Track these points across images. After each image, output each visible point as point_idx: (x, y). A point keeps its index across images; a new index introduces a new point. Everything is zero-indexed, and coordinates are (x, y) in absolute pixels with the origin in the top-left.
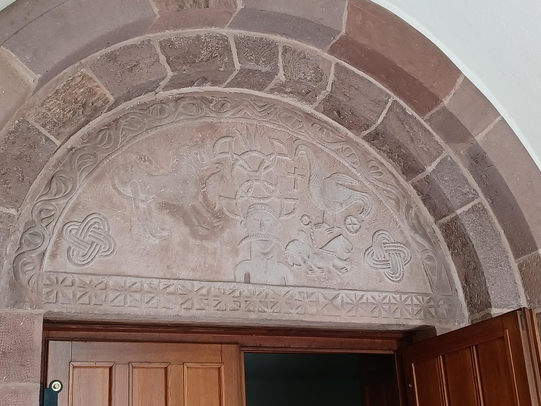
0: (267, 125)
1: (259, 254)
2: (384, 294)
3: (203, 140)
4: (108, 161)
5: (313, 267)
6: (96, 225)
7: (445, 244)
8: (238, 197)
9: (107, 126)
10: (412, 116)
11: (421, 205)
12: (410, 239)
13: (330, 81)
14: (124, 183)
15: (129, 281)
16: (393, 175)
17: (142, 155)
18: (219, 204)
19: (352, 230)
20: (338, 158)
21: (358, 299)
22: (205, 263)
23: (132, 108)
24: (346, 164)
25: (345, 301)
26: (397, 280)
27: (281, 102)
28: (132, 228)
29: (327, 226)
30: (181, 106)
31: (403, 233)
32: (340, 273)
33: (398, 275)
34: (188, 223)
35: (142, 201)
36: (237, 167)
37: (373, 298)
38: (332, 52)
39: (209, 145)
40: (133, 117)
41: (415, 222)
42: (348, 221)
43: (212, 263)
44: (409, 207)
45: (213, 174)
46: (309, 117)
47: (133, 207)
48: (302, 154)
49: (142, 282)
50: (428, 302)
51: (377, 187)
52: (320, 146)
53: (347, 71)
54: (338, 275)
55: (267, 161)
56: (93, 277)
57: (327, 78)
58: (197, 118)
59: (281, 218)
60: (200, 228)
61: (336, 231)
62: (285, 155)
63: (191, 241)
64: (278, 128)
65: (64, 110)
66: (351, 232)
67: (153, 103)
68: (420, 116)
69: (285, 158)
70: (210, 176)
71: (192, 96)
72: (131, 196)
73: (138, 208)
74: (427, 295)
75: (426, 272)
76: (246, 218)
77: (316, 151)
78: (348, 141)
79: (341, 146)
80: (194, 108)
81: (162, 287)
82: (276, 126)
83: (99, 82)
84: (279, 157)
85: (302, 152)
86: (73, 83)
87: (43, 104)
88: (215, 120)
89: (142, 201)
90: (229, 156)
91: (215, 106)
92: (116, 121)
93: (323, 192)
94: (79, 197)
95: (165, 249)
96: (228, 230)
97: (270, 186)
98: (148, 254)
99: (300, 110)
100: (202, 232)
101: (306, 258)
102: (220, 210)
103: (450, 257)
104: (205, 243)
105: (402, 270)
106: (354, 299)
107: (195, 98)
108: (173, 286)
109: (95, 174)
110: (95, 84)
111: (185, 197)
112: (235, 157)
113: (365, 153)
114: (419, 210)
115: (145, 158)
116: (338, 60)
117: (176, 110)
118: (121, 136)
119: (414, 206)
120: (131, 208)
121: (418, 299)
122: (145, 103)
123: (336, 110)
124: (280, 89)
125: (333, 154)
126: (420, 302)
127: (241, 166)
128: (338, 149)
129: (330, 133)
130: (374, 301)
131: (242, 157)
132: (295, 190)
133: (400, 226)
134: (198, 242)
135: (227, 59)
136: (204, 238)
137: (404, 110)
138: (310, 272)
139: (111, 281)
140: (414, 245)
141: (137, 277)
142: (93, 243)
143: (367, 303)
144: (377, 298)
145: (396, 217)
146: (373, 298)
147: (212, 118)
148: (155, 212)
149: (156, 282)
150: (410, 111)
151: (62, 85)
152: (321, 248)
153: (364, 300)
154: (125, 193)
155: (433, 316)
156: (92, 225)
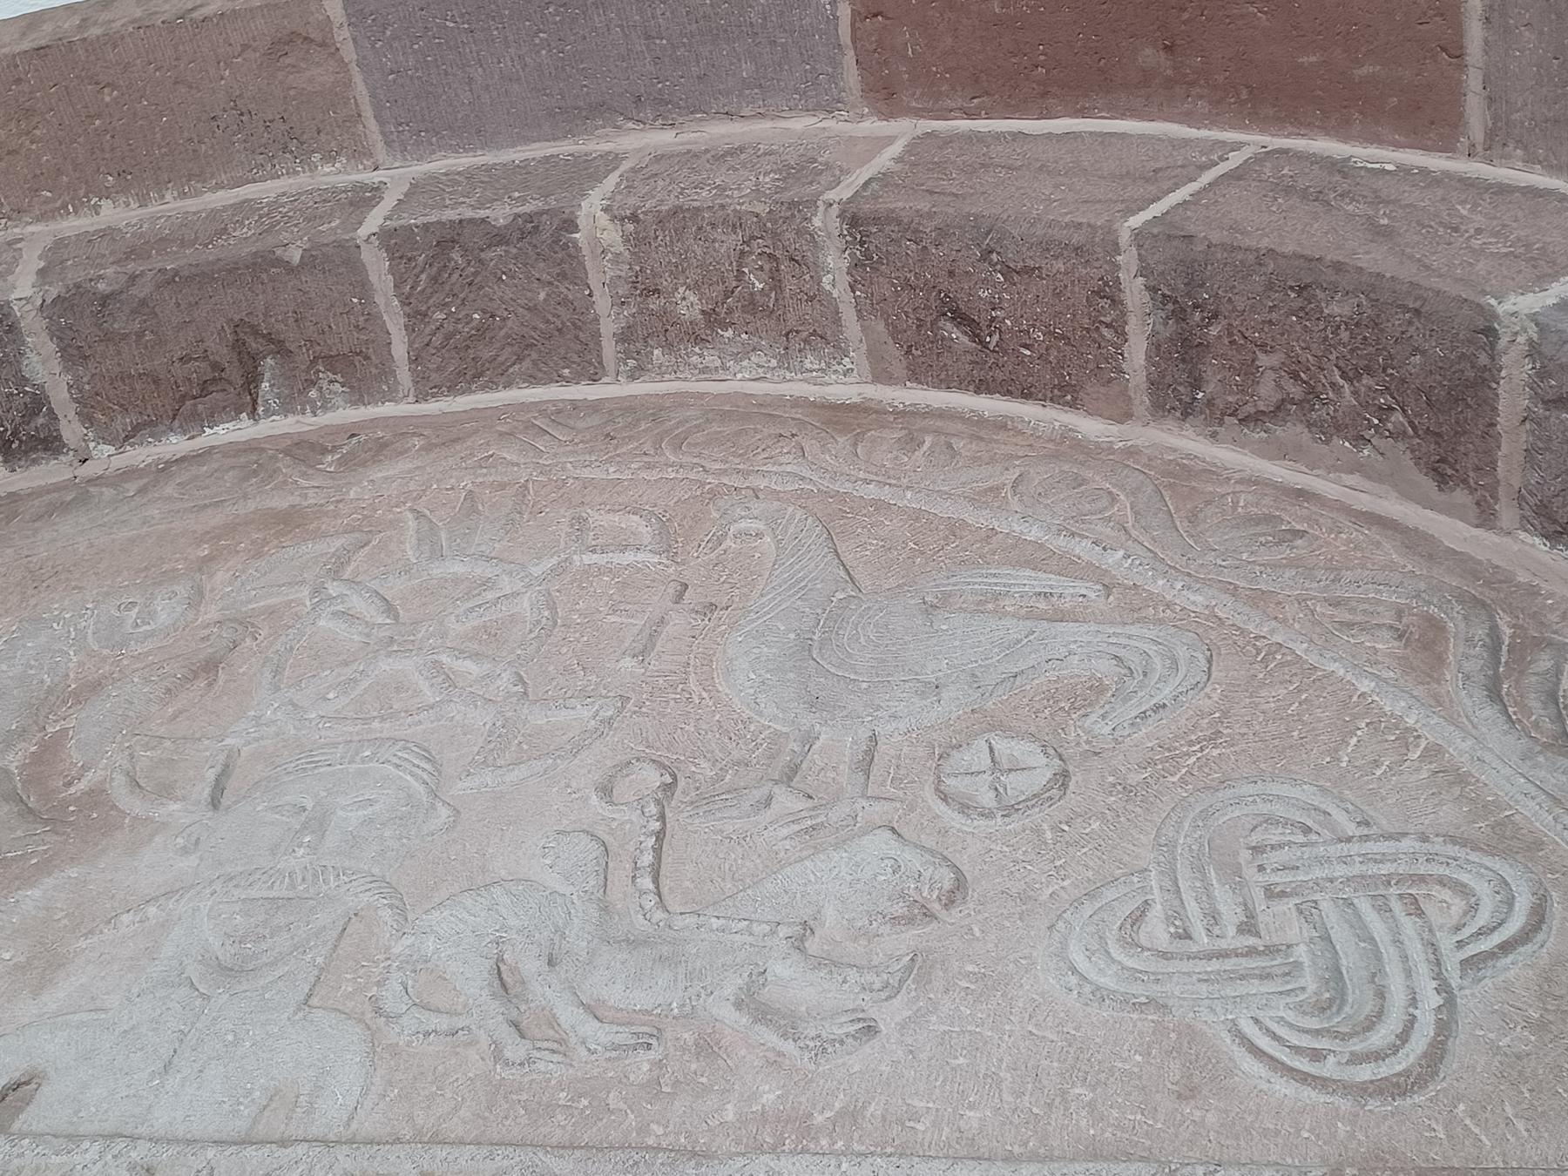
1: (193, 971)
5: (568, 1014)
26: (1365, 1073)
32: (788, 1046)
33: (1381, 1036)
64: (644, 475)
66: (964, 809)
101: (531, 966)
138: (515, 1049)
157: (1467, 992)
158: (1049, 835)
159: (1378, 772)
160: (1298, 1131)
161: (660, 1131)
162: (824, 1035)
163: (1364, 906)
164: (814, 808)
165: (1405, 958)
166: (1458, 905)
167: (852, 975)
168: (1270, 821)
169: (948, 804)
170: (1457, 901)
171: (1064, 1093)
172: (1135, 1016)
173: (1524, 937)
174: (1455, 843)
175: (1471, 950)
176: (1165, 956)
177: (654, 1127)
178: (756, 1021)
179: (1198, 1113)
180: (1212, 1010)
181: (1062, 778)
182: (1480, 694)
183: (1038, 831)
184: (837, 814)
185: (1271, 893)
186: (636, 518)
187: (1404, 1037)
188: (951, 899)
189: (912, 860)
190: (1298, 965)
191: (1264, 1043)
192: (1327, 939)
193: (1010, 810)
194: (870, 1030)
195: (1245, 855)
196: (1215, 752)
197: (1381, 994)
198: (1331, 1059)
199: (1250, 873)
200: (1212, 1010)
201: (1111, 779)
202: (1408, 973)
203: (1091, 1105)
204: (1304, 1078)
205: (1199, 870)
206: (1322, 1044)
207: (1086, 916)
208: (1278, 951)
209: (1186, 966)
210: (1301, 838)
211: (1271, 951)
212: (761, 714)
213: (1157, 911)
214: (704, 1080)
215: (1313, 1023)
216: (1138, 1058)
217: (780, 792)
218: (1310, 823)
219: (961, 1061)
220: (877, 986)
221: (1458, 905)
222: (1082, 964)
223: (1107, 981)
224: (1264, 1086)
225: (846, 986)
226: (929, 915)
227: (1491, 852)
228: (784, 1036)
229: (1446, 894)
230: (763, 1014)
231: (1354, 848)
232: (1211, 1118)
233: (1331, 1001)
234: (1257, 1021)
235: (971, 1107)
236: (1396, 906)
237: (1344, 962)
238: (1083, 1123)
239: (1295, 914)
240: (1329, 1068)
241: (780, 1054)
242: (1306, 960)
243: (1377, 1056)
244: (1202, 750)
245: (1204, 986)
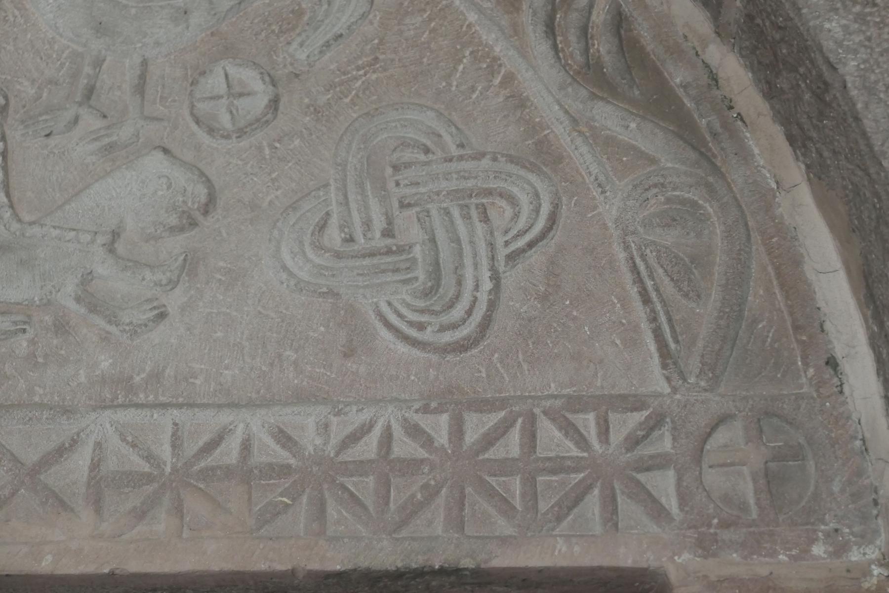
7: (777, 132)
12: (561, 132)
19: (225, 120)
21: (191, 448)
25: (111, 465)
26: (447, 337)
29: (90, 121)
32: (112, 329)
33: (458, 312)
37: (284, 438)
41: (604, 47)
42: (215, 82)
50: (633, 442)
54: (106, 338)
66: (211, 131)
74: (636, 403)
75: (639, 280)
103: (805, 195)
105: (487, 285)
106: (165, 452)
121: (570, 429)
126: (582, 442)
130: (284, 456)
133: (509, 79)
140: (582, 157)
143: (245, 473)
144: (310, 441)
145: (489, 36)
146: (284, 438)
152: (31, 224)
153: (229, 452)
155: (658, 512)
157: (508, 274)
158: (267, 151)
159: (474, 96)
160: (409, 376)
161: (41, 392)
162: (135, 321)
163: (456, 213)
164: (108, 127)
165: (475, 255)
166: (509, 212)
167: (148, 274)
168: (404, 144)
169: (199, 126)
170: (509, 208)
171: (280, 356)
172: (321, 300)
173: (543, 235)
174: (512, 162)
175: (513, 247)
176: (338, 255)
177: (37, 388)
178: (91, 311)
179: (355, 366)
180: (365, 297)
181: (274, 103)
182: (541, 28)
183: (260, 148)
184: (125, 133)
185: (403, 206)
187: (469, 313)
188: (207, 208)
189: (180, 177)
190: (414, 260)
191: (393, 319)
192: (433, 240)
193: (241, 133)
194: (162, 316)
195: (389, 171)
196: (374, 76)
197: (459, 283)
198: (429, 329)
199: (391, 185)
200: (365, 297)
201: (306, 101)
202: (476, 266)
203: (295, 363)
205: (361, 185)
206: (424, 318)
207: (291, 223)
208: (404, 250)
209: (351, 263)
210: (422, 157)
211: (401, 250)
212: (61, 36)
213: (334, 221)
214: (63, 352)
215: (421, 304)
216: (322, 329)
217: (83, 111)
218: (429, 143)
219: (219, 334)
220: (164, 282)
221: (509, 212)
222: (289, 263)
223: (304, 275)
224: (392, 346)
225: (144, 283)
226: (193, 224)
227: (533, 168)
228: (110, 322)
229: (503, 203)
230: (93, 308)
231: (454, 166)
232: (362, 369)
233: (432, 288)
234: (389, 304)
235: (227, 368)
236: (474, 213)
237: (442, 255)
238: (291, 375)
239: (415, 220)
240: (427, 336)
241: (108, 332)
242: (419, 256)
243: (454, 326)
244: (365, 75)
245: (360, 278)
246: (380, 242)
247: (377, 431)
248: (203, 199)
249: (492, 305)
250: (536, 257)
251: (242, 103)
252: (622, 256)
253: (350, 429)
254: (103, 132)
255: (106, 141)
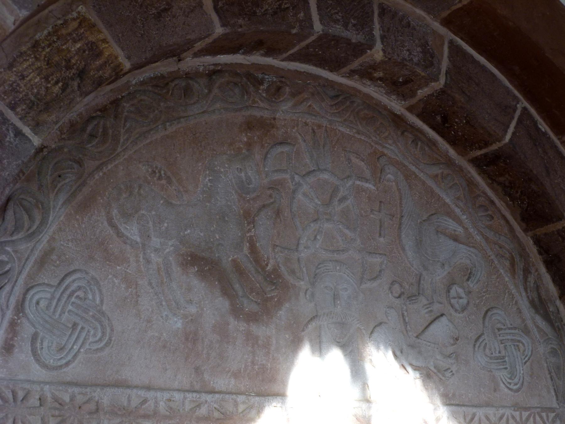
0: (341, 129)
2: (501, 411)
3: (249, 145)
4: (101, 174)
6: (80, 293)
8: (301, 248)
9: (100, 110)
10: (545, 134)
11: (543, 269)
12: (530, 324)
13: (444, 69)
14: (127, 216)
15: (136, 396)
16: (507, 221)
17: (156, 167)
18: (273, 258)
19: (457, 306)
20: (437, 190)
22: (253, 363)
23: (142, 83)
24: (448, 200)
27: (360, 92)
28: (140, 299)
30: (217, 85)
31: (520, 312)
32: (443, 378)
33: (516, 380)
34: (227, 291)
35: (156, 250)
36: (300, 196)
38: (447, 22)
39: (258, 157)
40: (143, 97)
41: (535, 295)
42: (453, 293)
43: (264, 362)
44: (527, 272)
45: (264, 206)
46: (397, 121)
47: (141, 259)
48: (389, 180)
49: (156, 398)
51: (487, 239)
52: (413, 168)
53: (465, 54)
55: (342, 189)
56: (76, 390)
57: (440, 62)
58: (241, 109)
59: (364, 286)
60: (245, 301)
61: (436, 307)
62: (367, 181)
63: (233, 323)
64: (356, 135)
65: (47, 78)
66: (456, 311)
67: (175, 76)
68: (556, 134)
69: (367, 185)
70: (260, 210)
71: (232, 70)
72: (138, 240)
73: (148, 262)
74: (552, 410)
76: (313, 284)
77: (408, 176)
78: (449, 163)
79: (440, 171)
80: (237, 91)
81: (188, 407)
82: (354, 131)
83: (106, 33)
84: (358, 182)
85: (391, 175)
86: (64, 32)
87: (11, 66)
88: (266, 114)
89: (156, 250)
90: (287, 176)
91: (267, 90)
92: (116, 103)
93: (419, 243)
94: (52, 239)
95: (191, 337)
96: (287, 305)
97: (347, 231)
98: (164, 347)
99: (385, 108)
100: (249, 306)
102: (275, 270)
104: (254, 328)
107: (237, 74)
108: (206, 406)
109: (80, 197)
110: (101, 36)
111: (222, 245)
112: (297, 178)
113: (471, 183)
114: (539, 277)
115: (160, 172)
116: (453, 36)
117: (210, 91)
118: (122, 131)
119: (533, 271)
120: (138, 261)
122: (162, 77)
123: (442, 116)
124: (366, 73)
125: (430, 183)
127: (305, 195)
128: (437, 176)
129: (427, 149)
131: (308, 179)
132: (382, 239)
134: (242, 326)
135: (302, 14)
136: (252, 318)
137: (535, 123)
139: (106, 397)
141: (148, 388)
142: (75, 325)
147: (261, 111)
148: (176, 270)
149: (177, 396)
150: (544, 126)
151: (46, 32)
154: (129, 235)
156: (73, 292)
168: (500, 322)
186: (363, 163)
191: (504, 380)
194: (453, 374)
195: (496, 331)
204: (508, 387)
240: (511, 387)
246: (498, 355)
247: (506, 416)
248: (458, 335)
249: (523, 377)
250: (528, 363)
251: (461, 301)
252: (545, 365)
253: (500, 415)
254: (428, 306)
255: (430, 309)
